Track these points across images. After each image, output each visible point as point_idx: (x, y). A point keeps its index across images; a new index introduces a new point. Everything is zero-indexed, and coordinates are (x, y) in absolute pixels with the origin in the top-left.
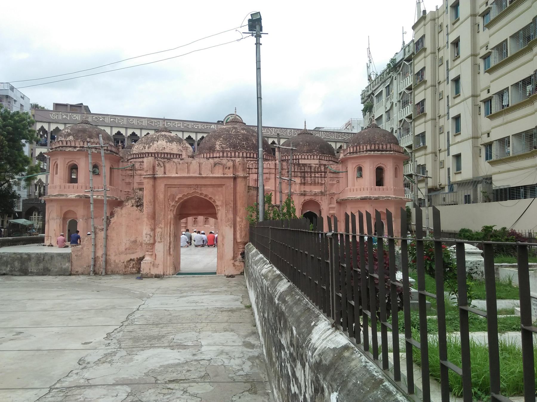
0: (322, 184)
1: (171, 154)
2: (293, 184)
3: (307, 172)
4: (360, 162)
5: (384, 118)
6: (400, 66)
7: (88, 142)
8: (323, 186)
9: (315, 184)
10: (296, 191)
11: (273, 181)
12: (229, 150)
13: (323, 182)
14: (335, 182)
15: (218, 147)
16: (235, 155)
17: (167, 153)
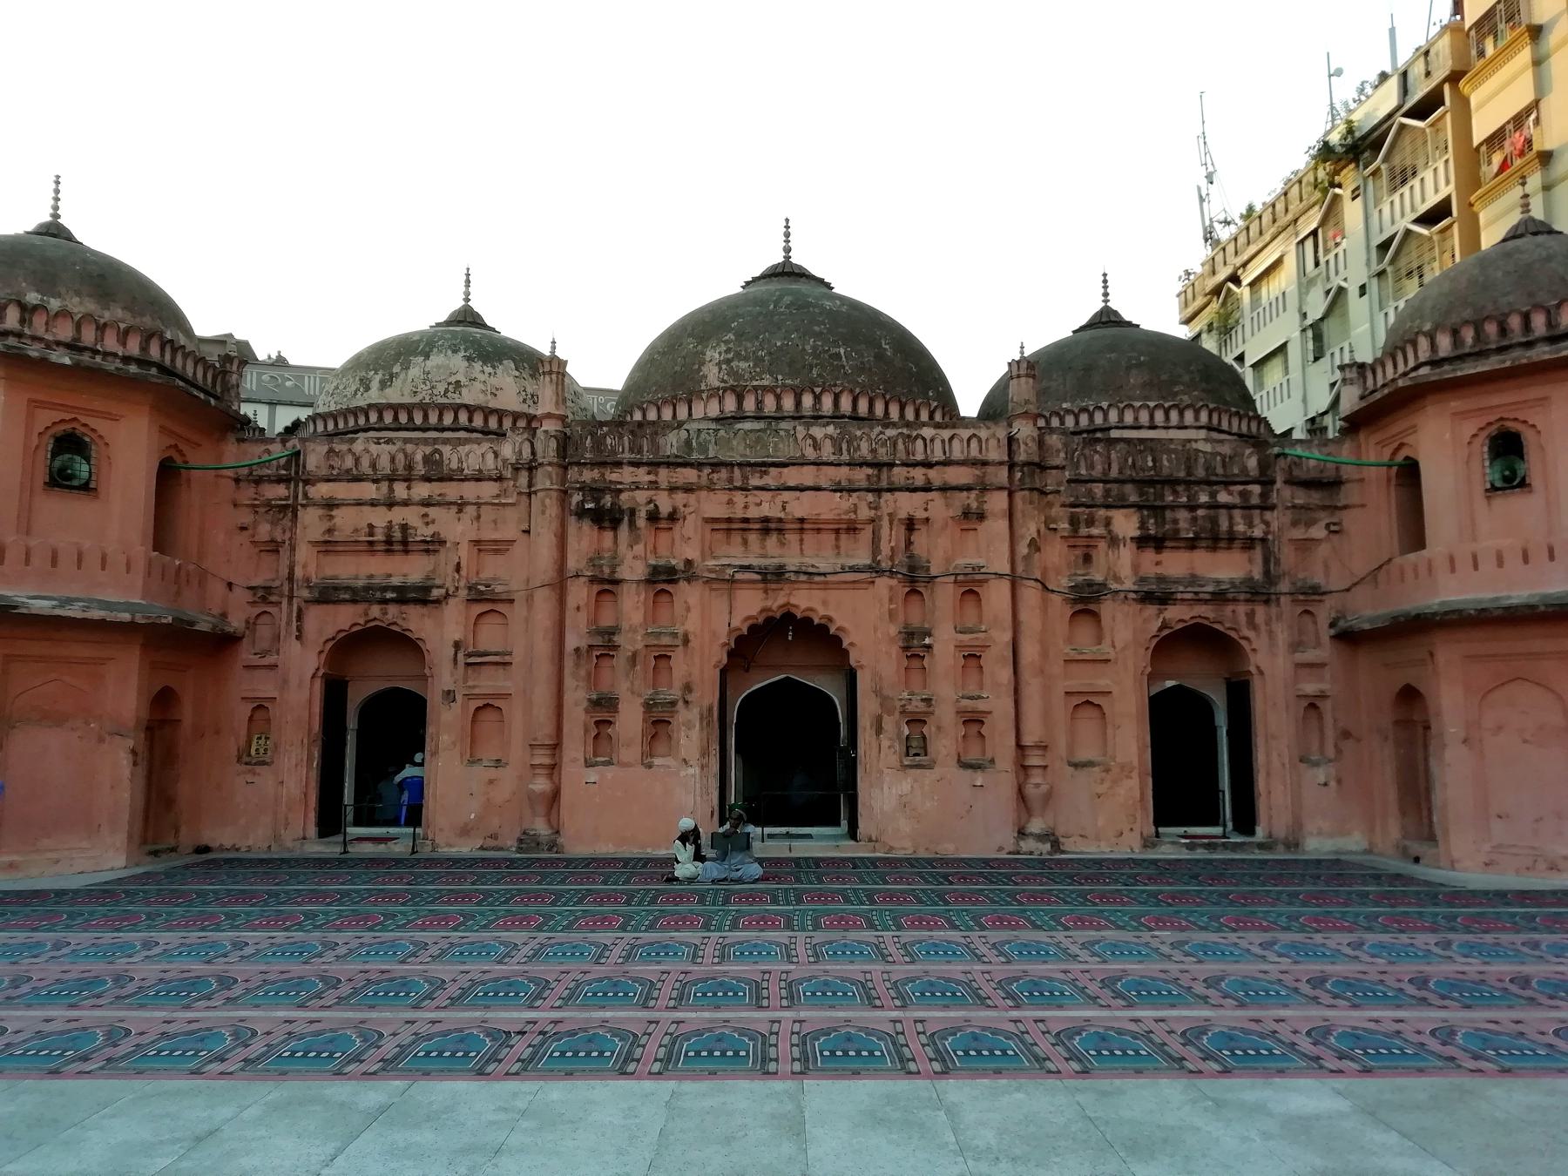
0: (1249, 543)
1: (488, 412)
2: (1102, 545)
3: (1172, 482)
4: (1502, 403)
5: (1294, 352)
6: (1377, 146)
7: (27, 311)
8: (1258, 553)
9: (1215, 540)
10: (1117, 579)
11: (1003, 524)
12: (765, 383)
13: (1258, 532)
14: (1318, 532)
15: (712, 375)
16: (798, 404)
17: (471, 410)
